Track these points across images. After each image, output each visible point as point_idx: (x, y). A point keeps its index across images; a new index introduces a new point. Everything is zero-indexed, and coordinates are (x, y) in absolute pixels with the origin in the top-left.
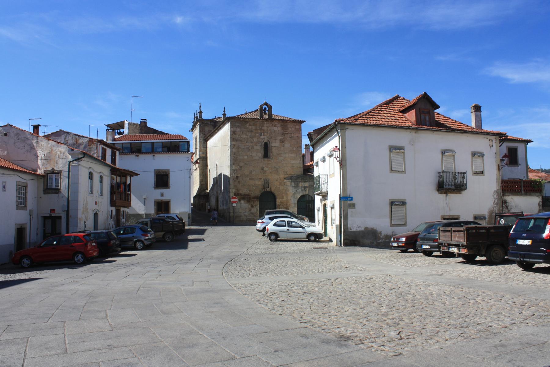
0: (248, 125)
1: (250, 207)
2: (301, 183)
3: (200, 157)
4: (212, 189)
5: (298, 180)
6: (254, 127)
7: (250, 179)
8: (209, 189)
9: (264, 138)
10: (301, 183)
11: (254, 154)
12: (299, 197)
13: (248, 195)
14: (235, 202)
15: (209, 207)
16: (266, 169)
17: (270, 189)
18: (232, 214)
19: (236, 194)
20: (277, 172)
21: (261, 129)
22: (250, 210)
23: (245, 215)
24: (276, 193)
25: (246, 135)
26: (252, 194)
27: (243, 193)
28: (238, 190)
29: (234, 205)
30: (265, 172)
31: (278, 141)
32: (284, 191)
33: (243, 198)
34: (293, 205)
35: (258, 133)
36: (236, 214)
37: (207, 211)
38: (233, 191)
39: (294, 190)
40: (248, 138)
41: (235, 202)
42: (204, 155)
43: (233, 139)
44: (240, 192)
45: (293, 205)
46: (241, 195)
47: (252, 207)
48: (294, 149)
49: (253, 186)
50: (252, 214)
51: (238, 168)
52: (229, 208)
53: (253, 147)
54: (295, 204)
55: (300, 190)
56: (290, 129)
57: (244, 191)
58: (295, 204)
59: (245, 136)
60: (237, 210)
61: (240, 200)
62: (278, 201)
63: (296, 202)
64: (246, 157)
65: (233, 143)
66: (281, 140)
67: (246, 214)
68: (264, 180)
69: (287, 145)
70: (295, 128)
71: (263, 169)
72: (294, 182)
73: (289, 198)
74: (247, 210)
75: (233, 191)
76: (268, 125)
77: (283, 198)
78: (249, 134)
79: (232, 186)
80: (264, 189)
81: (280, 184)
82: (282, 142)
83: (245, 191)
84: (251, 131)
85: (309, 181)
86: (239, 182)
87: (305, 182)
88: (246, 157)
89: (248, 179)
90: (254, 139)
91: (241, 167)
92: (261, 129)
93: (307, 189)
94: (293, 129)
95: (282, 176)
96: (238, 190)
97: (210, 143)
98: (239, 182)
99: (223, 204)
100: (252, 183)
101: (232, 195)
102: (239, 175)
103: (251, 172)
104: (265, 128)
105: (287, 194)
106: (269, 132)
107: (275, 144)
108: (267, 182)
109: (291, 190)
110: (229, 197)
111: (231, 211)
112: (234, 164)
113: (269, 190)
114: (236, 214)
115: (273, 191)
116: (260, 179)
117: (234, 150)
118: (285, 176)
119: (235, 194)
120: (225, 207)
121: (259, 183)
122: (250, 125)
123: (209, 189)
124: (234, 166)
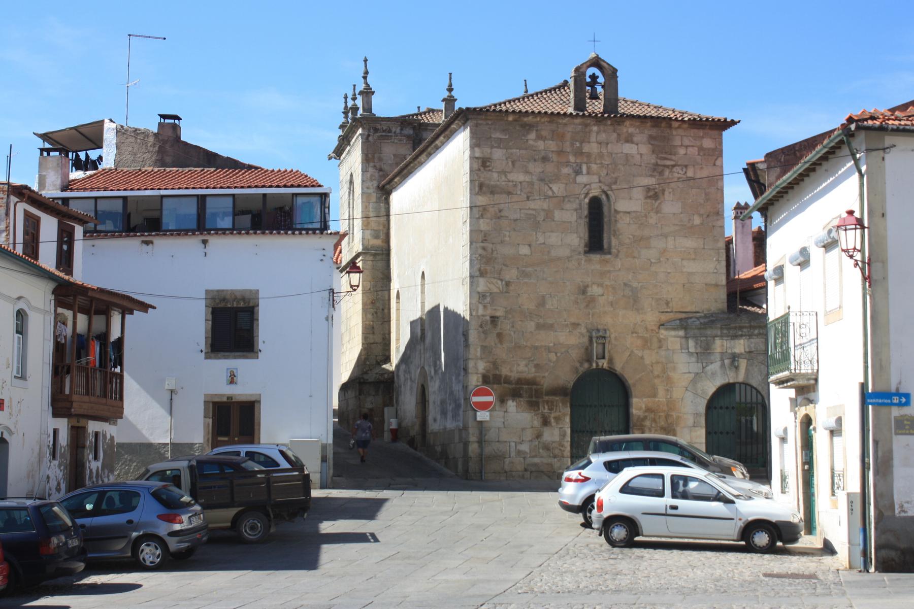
0: (532, 136)
1: (537, 423)
2: (718, 342)
3: (365, 247)
4: (405, 359)
5: (709, 332)
6: (552, 145)
7: (539, 327)
8: (395, 358)
9: (590, 183)
10: (718, 342)
11: (554, 239)
13: (531, 382)
14: (484, 406)
15: (393, 424)
16: (595, 290)
17: (611, 361)
18: (473, 448)
19: (490, 379)
20: (634, 302)
21: (579, 153)
22: (539, 436)
23: (519, 452)
24: (630, 378)
25: (527, 172)
26: (547, 380)
27: (514, 375)
28: (495, 364)
29: (483, 416)
30: (592, 301)
31: (638, 194)
32: (657, 370)
33: (515, 394)
34: (690, 421)
35: (567, 164)
36: (488, 450)
37: (387, 436)
38: (478, 367)
39: (695, 367)
40: (531, 184)
41: (484, 406)
42: (378, 242)
43: (481, 186)
44: (504, 371)
46: (507, 381)
47: (546, 422)
48: (697, 221)
49: (549, 350)
50: (547, 448)
51: (496, 286)
52: (465, 428)
53: (549, 215)
54: (697, 415)
55: (715, 367)
56: (682, 151)
58: (697, 415)
60: (491, 435)
61: (502, 400)
62: (638, 406)
63: (702, 409)
64: (524, 250)
65: (482, 200)
66: (648, 189)
67: (525, 447)
68: (589, 331)
69: (670, 206)
70: (701, 149)
71: (583, 290)
72: (695, 337)
73: (677, 393)
74: (529, 435)
75: (478, 367)
76: (603, 137)
77: (655, 395)
78: (536, 168)
79: (475, 351)
80: (589, 360)
81: (646, 343)
82: (653, 195)
83: (522, 368)
84: (545, 159)
85: (750, 336)
86: (500, 336)
87: (735, 337)
88: (524, 250)
89: (531, 325)
90: (555, 187)
91: (508, 284)
92: (579, 153)
93: (743, 363)
94: (693, 151)
95: (651, 318)
96: (495, 364)
97: (399, 199)
98: (500, 336)
99: (444, 413)
100: (546, 339)
101: (474, 380)
102: (500, 313)
103: (542, 302)
104: (592, 147)
105: (669, 380)
106: (607, 161)
107: (626, 205)
108: (598, 338)
109: (683, 365)
110: (465, 387)
111: (473, 439)
112: (482, 274)
113: (604, 364)
114: (488, 450)
115: (618, 367)
116: (575, 325)
117: (484, 225)
118: (664, 317)
119: (486, 379)
120: (450, 424)
121: (572, 341)
122: (540, 137)
123: (395, 358)
124: (482, 281)
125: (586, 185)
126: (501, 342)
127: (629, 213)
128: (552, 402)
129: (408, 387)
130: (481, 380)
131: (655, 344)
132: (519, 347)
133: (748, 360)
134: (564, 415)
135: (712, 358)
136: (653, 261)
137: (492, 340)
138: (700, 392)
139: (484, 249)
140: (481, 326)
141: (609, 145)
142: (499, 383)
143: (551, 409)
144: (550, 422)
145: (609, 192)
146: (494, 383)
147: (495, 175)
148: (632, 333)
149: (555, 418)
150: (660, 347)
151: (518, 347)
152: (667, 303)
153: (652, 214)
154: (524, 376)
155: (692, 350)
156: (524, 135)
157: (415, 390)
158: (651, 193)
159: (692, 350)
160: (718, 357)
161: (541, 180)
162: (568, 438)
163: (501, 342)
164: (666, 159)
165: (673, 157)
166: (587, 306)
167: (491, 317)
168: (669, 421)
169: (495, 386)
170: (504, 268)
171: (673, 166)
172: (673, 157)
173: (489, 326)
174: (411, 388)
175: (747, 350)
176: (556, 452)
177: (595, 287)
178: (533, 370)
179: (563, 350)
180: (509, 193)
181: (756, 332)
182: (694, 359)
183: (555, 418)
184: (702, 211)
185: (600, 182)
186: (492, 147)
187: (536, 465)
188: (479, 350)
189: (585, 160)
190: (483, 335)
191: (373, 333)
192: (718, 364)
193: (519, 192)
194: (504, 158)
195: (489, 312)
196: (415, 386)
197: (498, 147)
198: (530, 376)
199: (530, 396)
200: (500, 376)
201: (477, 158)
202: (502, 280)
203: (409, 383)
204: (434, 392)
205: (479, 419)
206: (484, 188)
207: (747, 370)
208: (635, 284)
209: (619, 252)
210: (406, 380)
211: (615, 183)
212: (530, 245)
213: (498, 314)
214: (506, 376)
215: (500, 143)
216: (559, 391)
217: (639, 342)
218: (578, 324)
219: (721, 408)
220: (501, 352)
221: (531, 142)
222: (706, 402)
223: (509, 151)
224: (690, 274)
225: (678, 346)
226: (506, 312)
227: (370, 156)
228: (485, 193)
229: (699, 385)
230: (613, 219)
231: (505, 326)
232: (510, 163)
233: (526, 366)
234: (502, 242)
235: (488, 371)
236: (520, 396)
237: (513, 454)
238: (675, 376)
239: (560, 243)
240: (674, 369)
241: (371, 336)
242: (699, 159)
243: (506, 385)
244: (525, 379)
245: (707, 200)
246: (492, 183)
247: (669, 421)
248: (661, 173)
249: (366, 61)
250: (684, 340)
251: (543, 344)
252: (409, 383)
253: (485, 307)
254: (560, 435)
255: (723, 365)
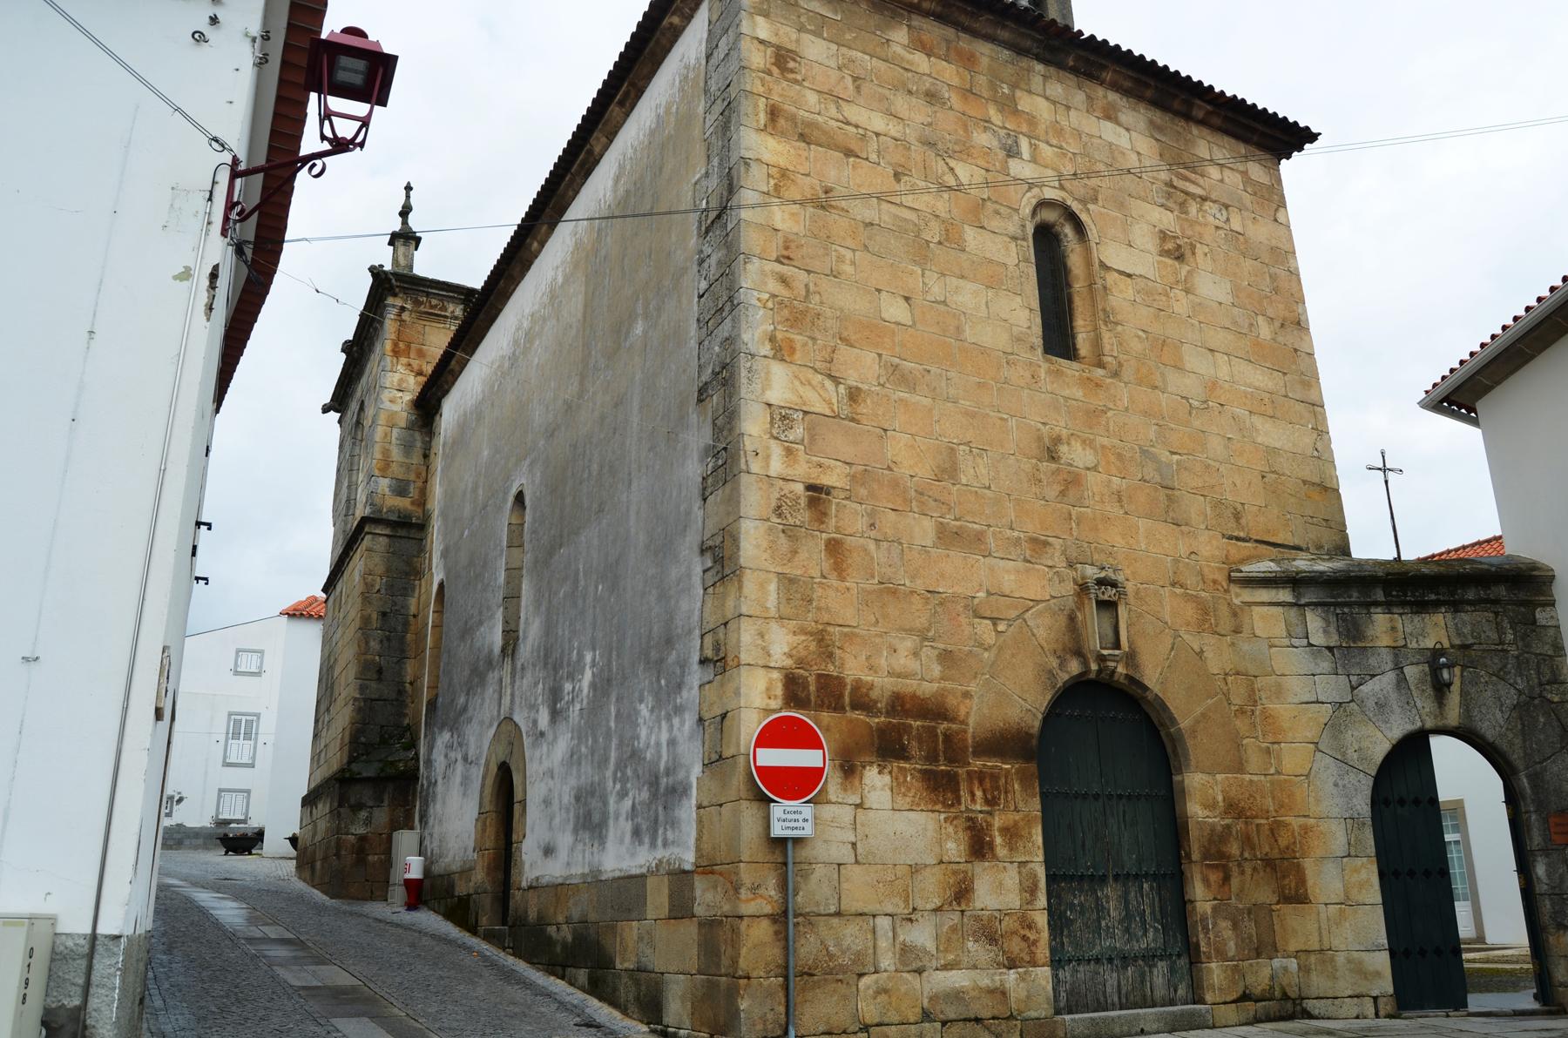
1: (955, 848)
7: (949, 537)
11: (968, 296)
12: (1380, 748)
13: (933, 710)
15: (414, 867)
16: (1077, 455)
19: (811, 691)
22: (962, 892)
23: (906, 952)
27: (882, 685)
28: (823, 642)
30: (1072, 481)
31: (1144, 238)
33: (889, 748)
39: (1332, 687)
41: (799, 783)
44: (852, 668)
45: (1338, 838)
46: (862, 703)
47: (979, 847)
48: (1265, 331)
51: (821, 397)
53: (951, 238)
55: (1382, 685)
56: (1214, 172)
57: (888, 663)
58: (1352, 820)
59: (878, 122)
62: (1203, 795)
63: (1362, 805)
64: (895, 310)
66: (1164, 236)
67: (922, 935)
69: (1212, 287)
73: (1294, 758)
74: (931, 890)
77: (1239, 767)
78: (916, 113)
79: (759, 590)
82: (1176, 251)
83: (903, 661)
84: (932, 97)
85: (1456, 606)
88: (895, 310)
89: (923, 530)
91: (854, 395)
96: (823, 642)
99: (591, 824)
100: (964, 575)
102: (833, 478)
103: (948, 471)
119: (794, 690)
120: (620, 856)
121: (1038, 587)
125: (1031, 186)
126: (839, 569)
127: (1129, 276)
128: (995, 778)
129: (458, 779)
130: (779, 690)
131: (1226, 624)
132: (894, 592)
133: (1464, 667)
134: (1029, 822)
135: (1373, 661)
136: (1196, 404)
137: (812, 560)
138: (1352, 756)
139: (784, 280)
140: (778, 511)
141: (1072, 113)
142: (838, 707)
143: (991, 802)
144: (991, 846)
145: (1084, 217)
146: (821, 706)
147: (812, 98)
148: (1173, 585)
149: (1005, 831)
150: (1237, 631)
151: (889, 590)
152: (1237, 516)
153: (1178, 293)
154: (910, 686)
155: (1318, 638)
156: (878, 27)
157: (477, 785)
158: (1170, 246)
159: (1318, 638)
160: (1387, 659)
161: (931, 144)
162: (1042, 901)
163: (839, 569)
164: (1186, 179)
165: (1201, 181)
166: (1063, 493)
167: (810, 487)
168: (1283, 842)
169: (826, 716)
170: (842, 347)
171: (1204, 199)
172: (1201, 181)
173: (803, 516)
174: (466, 781)
175: (1457, 642)
176: (1016, 946)
177: (1077, 445)
178: (936, 670)
179: (1013, 614)
180: (849, 153)
181: (1471, 595)
182: (1326, 665)
183: (1005, 831)
184: (1270, 312)
185: (1062, 188)
186: (802, 29)
187: (957, 996)
188: (773, 587)
189: (1024, 128)
190: (783, 539)
191: (379, 680)
192: (1390, 677)
193: (873, 157)
194: (833, 64)
195: (803, 470)
196: (477, 773)
197: (817, 34)
198: (927, 689)
199: (932, 757)
200: (840, 681)
201: (762, 42)
202: (836, 381)
203: (460, 767)
204: (550, 773)
205: (777, 831)
206: (782, 122)
207: (1464, 694)
208: (1164, 456)
209: (1120, 365)
210: (450, 765)
211: (1095, 200)
212: (907, 299)
213: (826, 480)
214: (858, 685)
215: (819, 27)
216: (1002, 743)
217: (1190, 612)
218: (1046, 544)
219: (1402, 802)
220: (841, 603)
221: (899, 50)
222: (1370, 782)
223: (844, 50)
224: (1272, 451)
225: (1280, 630)
226: (853, 478)
227: (401, 345)
228: (783, 134)
229: (1349, 736)
230: (1099, 282)
231: (849, 519)
232: (849, 80)
233: (916, 654)
234: (834, 274)
235: (801, 663)
236: (901, 754)
237: (887, 961)
238: (1282, 710)
239: (983, 312)
240: (1279, 692)
241: (374, 685)
242: (1247, 199)
243: (858, 715)
244: (914, 696)
245: (1276, 290)
246: (802, 113)
247: (1283, 842)
248: (1183, 206)
249: (408, 188)
250: (1293, 612)
251: (958, 589)
252: (460, 767)
253: (789, 452)
254: (1022, 890)
255: (1402, 682)
